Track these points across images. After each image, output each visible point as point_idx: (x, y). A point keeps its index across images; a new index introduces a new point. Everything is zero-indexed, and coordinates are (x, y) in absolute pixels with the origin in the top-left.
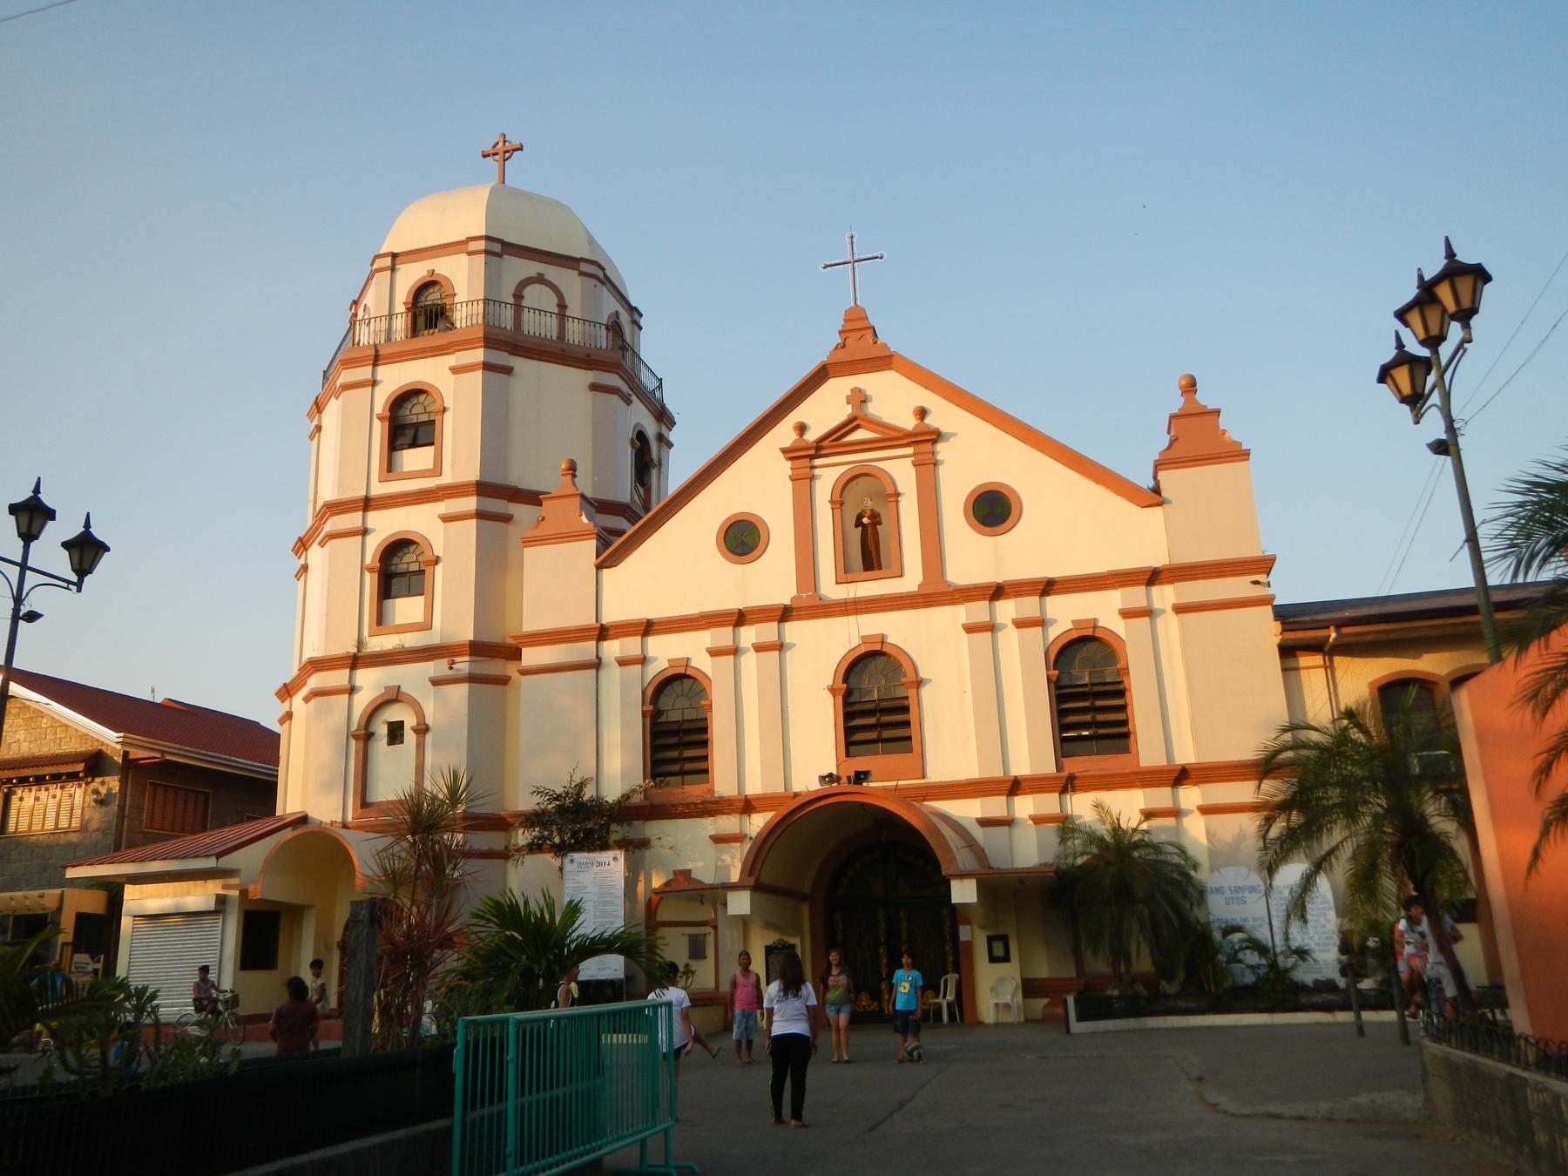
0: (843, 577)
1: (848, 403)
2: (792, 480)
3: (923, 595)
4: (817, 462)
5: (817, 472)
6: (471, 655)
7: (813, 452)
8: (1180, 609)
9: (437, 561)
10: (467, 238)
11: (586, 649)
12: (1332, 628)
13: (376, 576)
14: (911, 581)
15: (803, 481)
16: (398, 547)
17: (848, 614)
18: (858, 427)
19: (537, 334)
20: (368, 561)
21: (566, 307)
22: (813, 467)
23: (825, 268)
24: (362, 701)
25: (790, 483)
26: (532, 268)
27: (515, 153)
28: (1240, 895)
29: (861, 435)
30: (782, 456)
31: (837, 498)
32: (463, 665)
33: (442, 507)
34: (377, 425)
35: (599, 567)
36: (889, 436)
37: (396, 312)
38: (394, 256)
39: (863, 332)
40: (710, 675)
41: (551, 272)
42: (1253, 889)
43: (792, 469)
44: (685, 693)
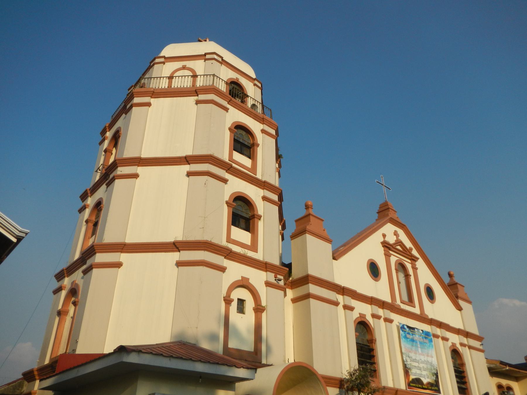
1: (394, 235)
3: (420, 316)
9: (259, 217)
12: (507, 366)
13: (231, 210)
14: (417, 310)
15: (387, 256)
20: (227, 198)
23: (377, 182)
25: (384, 256)
29: (399, 247)
36: (405, 252)
38: (222, 60)
39: (394, 212)
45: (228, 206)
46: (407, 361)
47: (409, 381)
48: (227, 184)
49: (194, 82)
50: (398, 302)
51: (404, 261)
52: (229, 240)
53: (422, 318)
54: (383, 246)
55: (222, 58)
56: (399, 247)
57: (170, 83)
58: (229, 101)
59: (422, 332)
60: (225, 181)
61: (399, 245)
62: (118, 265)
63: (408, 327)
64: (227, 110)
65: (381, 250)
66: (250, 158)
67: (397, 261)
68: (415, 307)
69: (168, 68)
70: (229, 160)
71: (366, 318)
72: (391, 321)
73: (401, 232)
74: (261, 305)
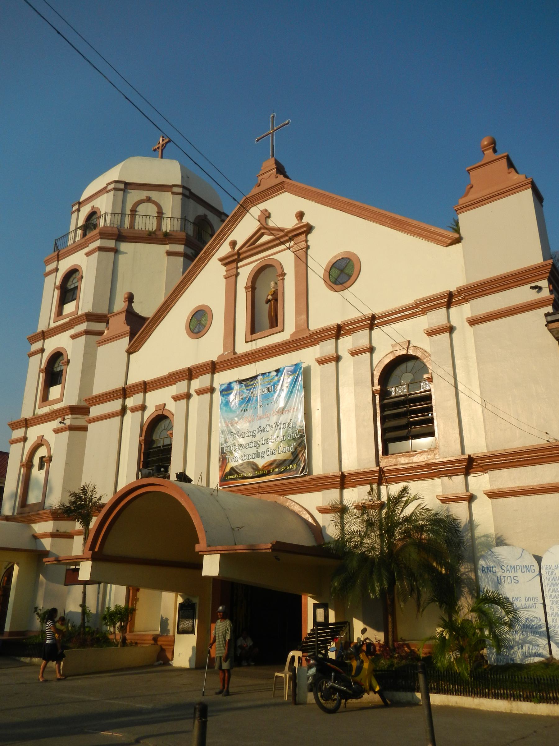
0: (250, 337)
2: (226, 278)
4: (240, 264)
5: (239, 270)
6: (72, 414)
7: (236, 257)
8: (473, 322)
10: (107, 184)
11: (115, 405)
16: (57, 356)
17: (250, 363)
18: (262, 235)
19: (144, 229)
20: (42, 367)
21: (162, 213)
22: (237, 268)
24: (29, 445)
26: (144, 194)
27: (168, 145)
28: (512, 575)
29: (266, 238)
30: (220, 263)
31: (250, 284)
32: (69, 420)
33: (72, 332)
34: (56, 291)
35: (130, 352)
37: (70, 231)
40: (174, 413)
41: (154, 195)
42: (527, 569)
43: (226, 271)
44: (166, 428)
46: (226, 442)
47: (225, 472)
54: (225, 265)
59: (275, 373)
63: (240, 382)
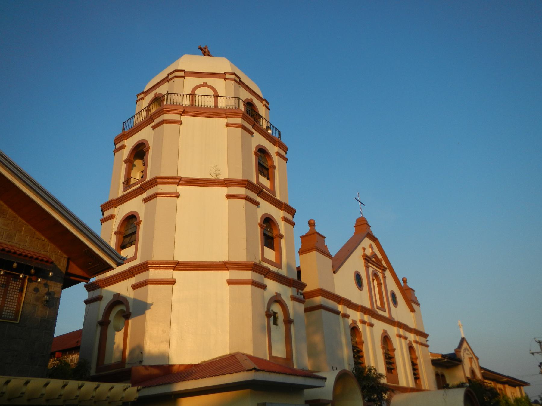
9: (281, 237)
14: (386, 315)
15: (367, 267)
23: (355, 199)
25: (364, 268)
29: (374, 259)
38: (240, 80)
45: (260, 227)
48: (260, 207)
49: (216, 102)
50: (375, 308)
51: (378, 272)
52: (265, 260)
53: (391, 321)
54: (363, 259)
55: (239, 78)
56: (374, 259)
57: (192, 101)
58: (252, 125)
60: (257, 204)
61: (374, 258)
62: (173, 282)
64: (251, 133)
65: (362, 261)
66: (269, 179)
67: (373, 271)
68: (385, 312)
69: (190, 83)
70: (256, 183)
71: (357, 324)
72: (371, 325)
73: (374, 245)
74: (289, 317)
